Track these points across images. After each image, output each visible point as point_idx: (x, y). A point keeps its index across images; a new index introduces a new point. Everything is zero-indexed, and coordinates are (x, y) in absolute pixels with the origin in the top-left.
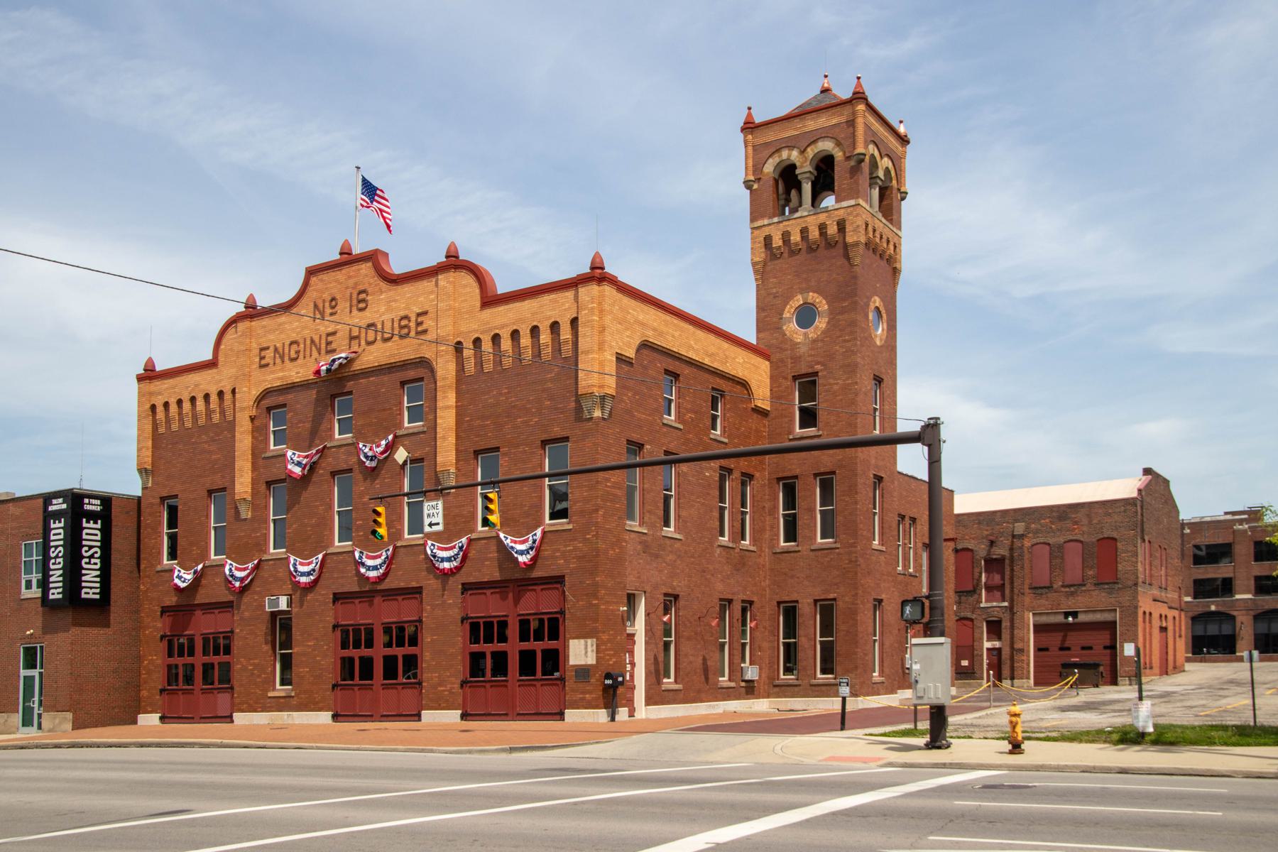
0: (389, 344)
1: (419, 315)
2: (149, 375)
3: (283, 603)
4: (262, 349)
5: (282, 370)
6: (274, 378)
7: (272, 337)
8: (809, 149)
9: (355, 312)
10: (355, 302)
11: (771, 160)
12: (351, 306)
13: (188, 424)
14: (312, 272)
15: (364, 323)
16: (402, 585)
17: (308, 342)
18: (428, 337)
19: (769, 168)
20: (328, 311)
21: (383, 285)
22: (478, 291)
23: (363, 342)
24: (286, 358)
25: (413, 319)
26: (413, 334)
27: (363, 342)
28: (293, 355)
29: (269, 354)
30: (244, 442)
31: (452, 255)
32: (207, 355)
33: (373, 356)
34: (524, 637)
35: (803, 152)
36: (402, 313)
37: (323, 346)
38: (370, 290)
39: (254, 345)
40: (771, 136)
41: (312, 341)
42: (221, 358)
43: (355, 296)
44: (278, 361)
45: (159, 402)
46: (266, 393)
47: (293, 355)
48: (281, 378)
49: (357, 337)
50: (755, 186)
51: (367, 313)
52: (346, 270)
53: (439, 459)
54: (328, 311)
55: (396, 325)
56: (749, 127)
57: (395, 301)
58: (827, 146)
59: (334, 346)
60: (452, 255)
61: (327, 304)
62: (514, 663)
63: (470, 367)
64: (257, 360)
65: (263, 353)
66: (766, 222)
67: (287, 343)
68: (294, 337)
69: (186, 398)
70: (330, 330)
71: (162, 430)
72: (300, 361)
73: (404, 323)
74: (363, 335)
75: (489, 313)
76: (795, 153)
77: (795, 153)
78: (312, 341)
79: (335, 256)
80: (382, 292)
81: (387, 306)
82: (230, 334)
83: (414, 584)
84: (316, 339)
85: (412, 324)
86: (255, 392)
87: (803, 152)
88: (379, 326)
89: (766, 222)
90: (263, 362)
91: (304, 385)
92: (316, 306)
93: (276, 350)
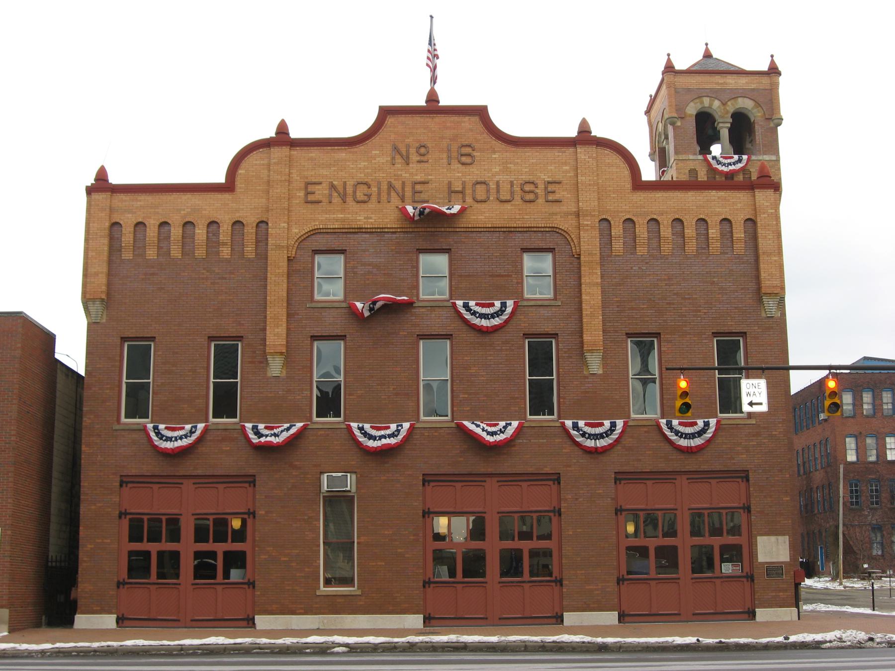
0: (508, 206)
1: (549, 183)
2: (101, 185)
3: (350, 483)
4: (308, 184)
5: (343, 211)
6: (332, 217)
7: (325, 172)
8: (729, 103)
9: (456, 165)
10: (454, 154)
11: (692, 104)
12: (449, 158)
13: (176, 252)
14: (386, 112)
15: (470, 179)
16: (530, 470)
17: (384, 187)
18: (564, 208)
19: (692, 110)
20: (414, 157)
21: (498, 145)
22: (626, 172)
23: (469, 200)
24: (349, 199)
25: (541, 186)
26: (541, 201)
27: (469, 200)
28: (360, 196)
29: (321, 192)
30: (277, 287)
31: (584, 129)
32: (221, 179)
33: (485, 215)
34: (696, 532)
35: (724, 104)
36: (525, 178)
37: (408, 193)
38: (477, 146)
39: (295, 176)
40: (694, 82)
41: (390, 186)
42: (239, 184)
43: (454, 147)
44: (336, 200)
45: (128, 221)
46: (316, 232)
47: (360, 196)
48: (343, 220)
49: (462, 192)
50: (679, 124)
51: (474, 169)
52: (439, 119)
53: (586, 337)
54: (414, 157)
55: (517, 189)
56: (669, 68)
57: (516, 164)
58: (745, 104)
59: (423, 196)
60: (584, 129)
61: (413, 151)
62: (685, 559)
63: (618, 246)
64: (302, 194)
65: (311, 188)
66: (691, 157)
67: (350, 183)
68: (361, 176)
69: (176, 222)
70: (418, 178)
71: (127, 255)
72: (372, 205)
73: (527, 188)
74: (468, 191)
75: (641, 197)
76: (716, 104)
77: (716, 104)
78: (390, 186)
79: (421, 101)
80: (494, 152)
81: (493, 166)
82: (253, 159)
83: (547, 470)
84: (398, 185)
85: (540, 191)
86: (297, 231)
87: (724, 104)
88: (493, 186)
89: (691, 157)
90: (311, 198)
91: (378, 232)
92: (396, 149)
93: (332, 187)
